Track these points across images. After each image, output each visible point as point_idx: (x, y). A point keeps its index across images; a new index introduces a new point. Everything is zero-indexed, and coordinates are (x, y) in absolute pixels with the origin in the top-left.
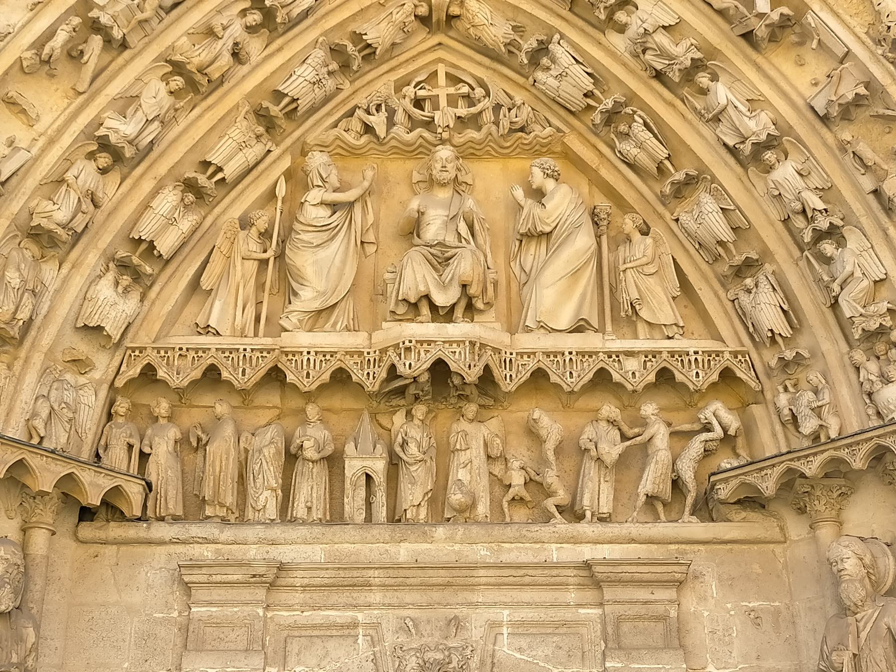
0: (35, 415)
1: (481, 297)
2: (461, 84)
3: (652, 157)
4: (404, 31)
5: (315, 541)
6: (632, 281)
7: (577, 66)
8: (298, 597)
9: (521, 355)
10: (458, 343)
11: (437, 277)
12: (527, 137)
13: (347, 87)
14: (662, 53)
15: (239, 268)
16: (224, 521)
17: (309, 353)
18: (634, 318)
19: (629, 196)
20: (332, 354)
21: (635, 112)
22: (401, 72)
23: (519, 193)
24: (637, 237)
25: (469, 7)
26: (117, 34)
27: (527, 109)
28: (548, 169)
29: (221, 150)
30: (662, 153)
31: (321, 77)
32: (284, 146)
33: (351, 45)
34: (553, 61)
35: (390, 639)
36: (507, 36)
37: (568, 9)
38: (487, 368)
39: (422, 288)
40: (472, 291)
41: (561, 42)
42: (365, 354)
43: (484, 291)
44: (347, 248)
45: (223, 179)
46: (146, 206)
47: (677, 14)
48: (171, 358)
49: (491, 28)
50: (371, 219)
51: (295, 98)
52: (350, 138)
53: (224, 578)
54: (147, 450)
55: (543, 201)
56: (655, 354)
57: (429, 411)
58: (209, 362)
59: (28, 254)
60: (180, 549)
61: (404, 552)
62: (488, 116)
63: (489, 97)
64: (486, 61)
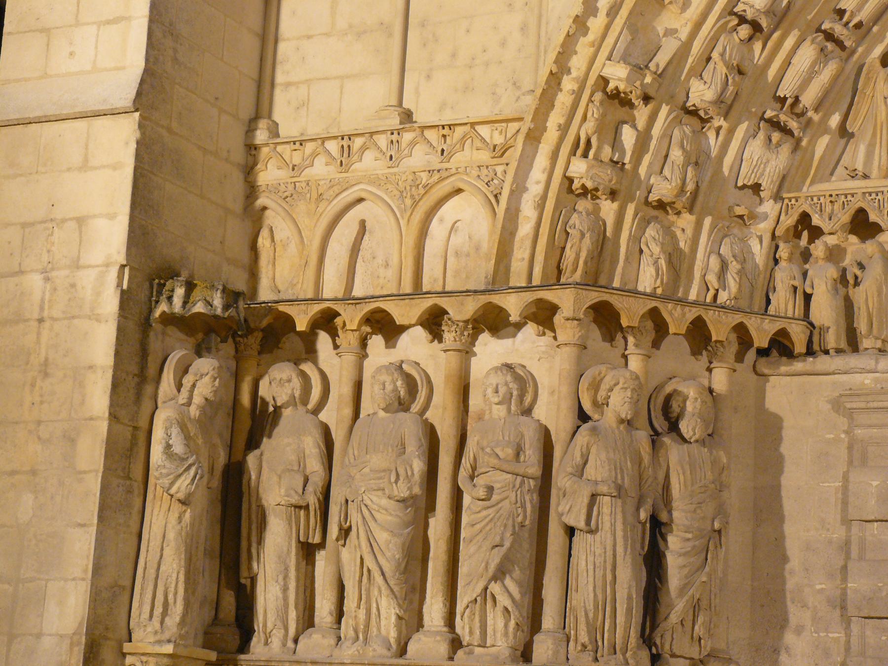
48: (823, 205)
53: (880, 404)
54: (809, 291)
58: (857, 206)
59: (687, 130)
60: (845, 378)
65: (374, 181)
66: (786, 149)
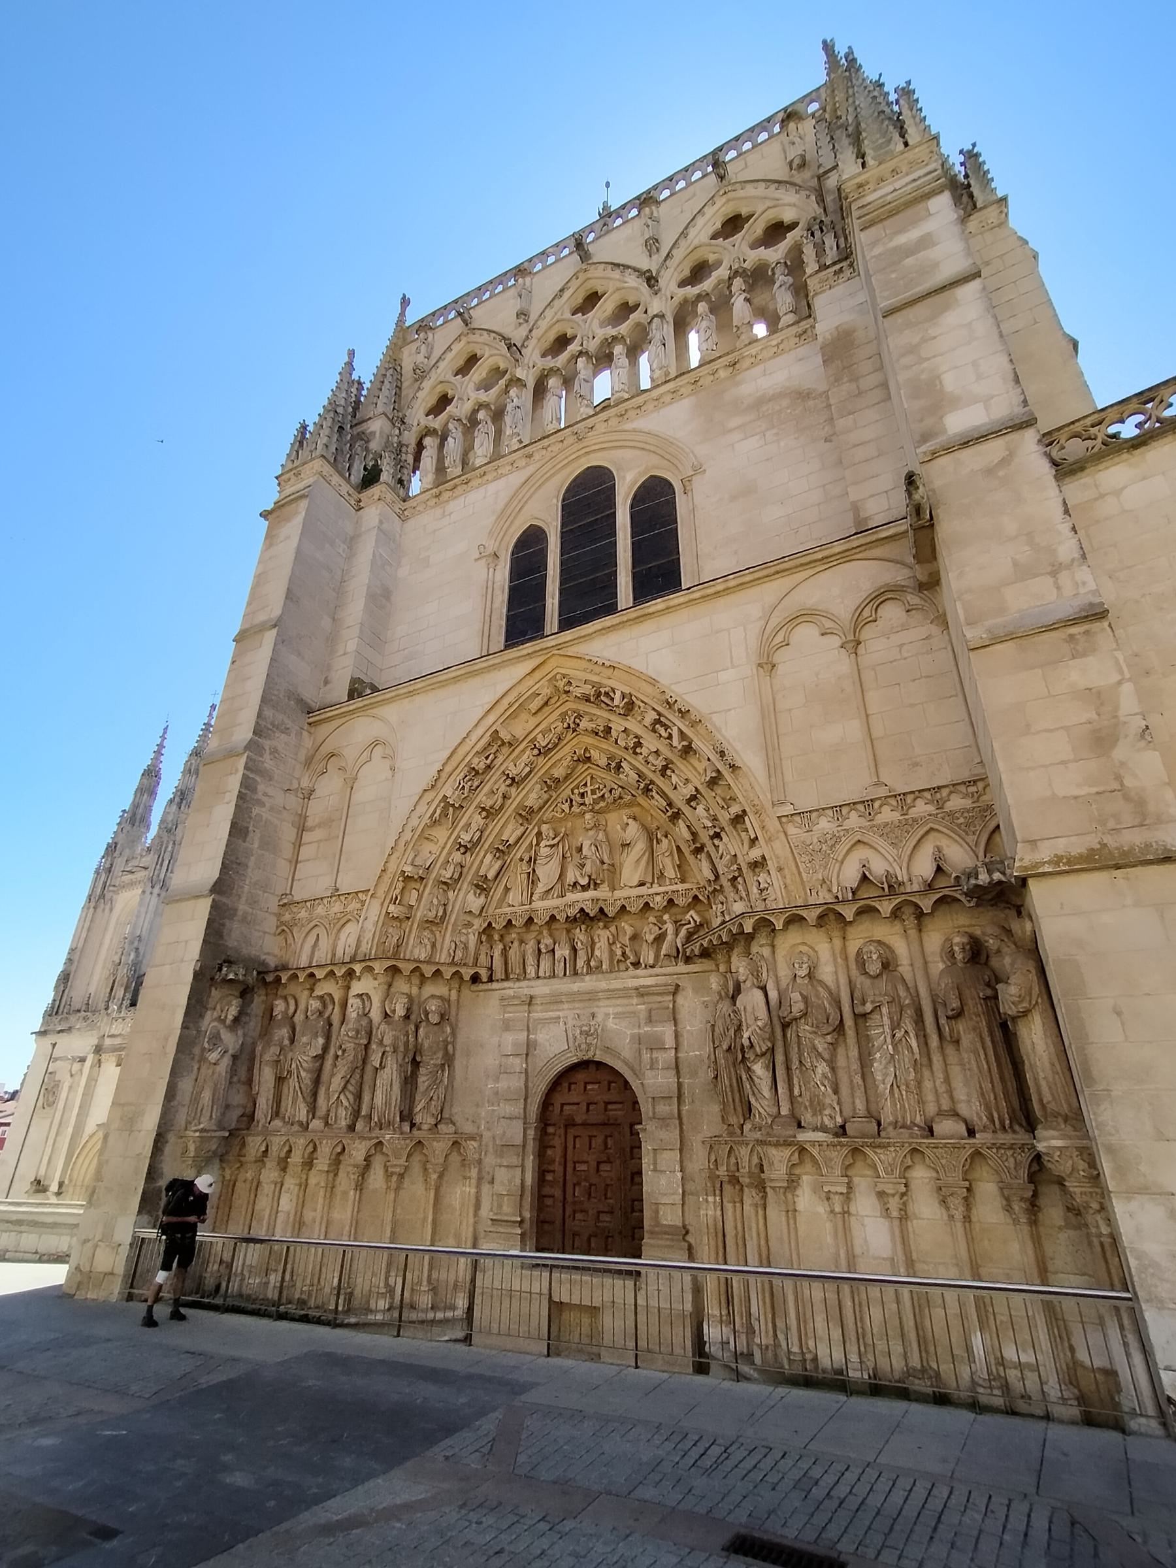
0: (450, 947)
5: (545, 985)
8: (539, 1008)
16: (518, 980)
24: (663, 839)
26: (457, 805)
35: (570, 1023)
39: (574, 880)
46: (482, 862)
61: (576, 986)
65: (321, 918)
66: (483, 897)
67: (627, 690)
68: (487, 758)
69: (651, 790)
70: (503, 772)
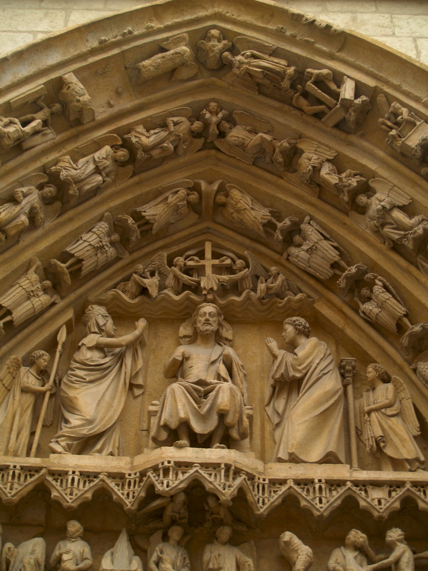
1: (236, 427)
2: (224, 258)
3: (391, 315)
4: (178, 213)
6: (376, 420)
7: (325, 242)
9: (273, 482)
10: (216, 466)
11: (198, 409)
12: (281, 301)
13: (127, 258)
14: (399, 226)
15: (17, 397)
17: (74, 472)
18: (378, 455)
19: (372, 352)
20: (96, 475)
21: (376, 278)
22: (175, 249)
23: (274, 344)
25: (233, 196)
27: (281, 278)
28: (299, 326)
29: (11, 296)
30: (400, 310)
31: (104, 243)
32: (67, 300)
33: (131, 219)
34: (305, 239)
36: (265, 217)
37: (316, 196)
38: (241, 490)
39: (182, 415)
40: (229, 419)
41: (311, 222)
42: (127, 476)
43: (240, 421)
44: (117, 387)
45: (11, 322)
47: (410, 196)
49: (252, 211)
50: (140, 364)
51: (80, 258)
52: (125, 297)
55: (296, 351)
56: (400, 484)
57: (185, 534)
62: (248, 283)
63: (249, 268)
64: (248, 242)
67: (371, 82)
68: (25, 124)
69: (371, 285)
70: (44, 169)
